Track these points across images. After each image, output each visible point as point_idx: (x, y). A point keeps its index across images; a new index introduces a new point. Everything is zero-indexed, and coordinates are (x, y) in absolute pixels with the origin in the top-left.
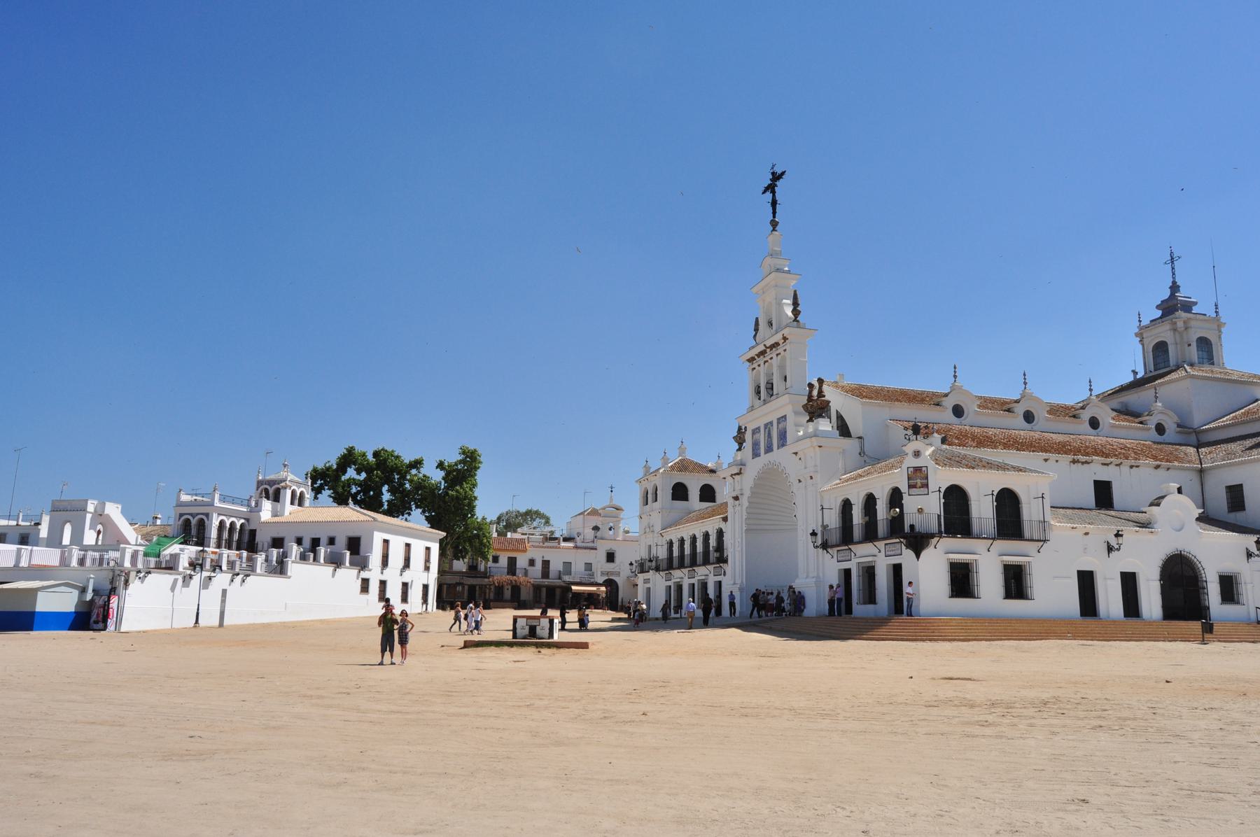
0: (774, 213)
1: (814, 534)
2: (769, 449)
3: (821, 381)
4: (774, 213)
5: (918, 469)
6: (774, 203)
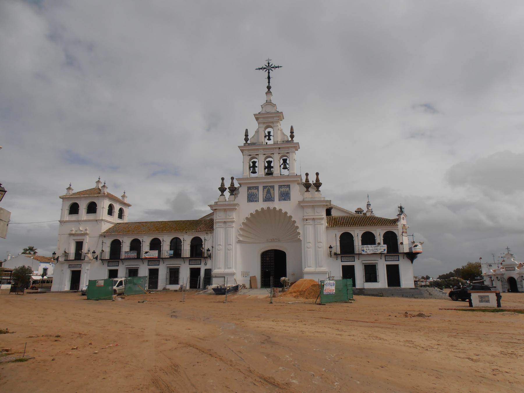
0: (269, 82)
1: (331, 247)
2: (269, 198)
3: (317, 174)
4: (269, 82)
5: (404, 225)
6: (269, 78)
